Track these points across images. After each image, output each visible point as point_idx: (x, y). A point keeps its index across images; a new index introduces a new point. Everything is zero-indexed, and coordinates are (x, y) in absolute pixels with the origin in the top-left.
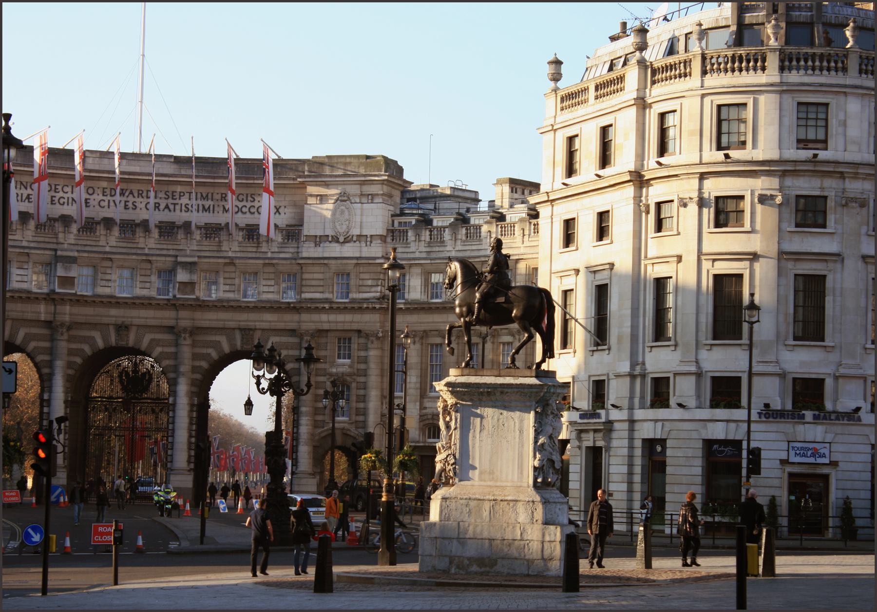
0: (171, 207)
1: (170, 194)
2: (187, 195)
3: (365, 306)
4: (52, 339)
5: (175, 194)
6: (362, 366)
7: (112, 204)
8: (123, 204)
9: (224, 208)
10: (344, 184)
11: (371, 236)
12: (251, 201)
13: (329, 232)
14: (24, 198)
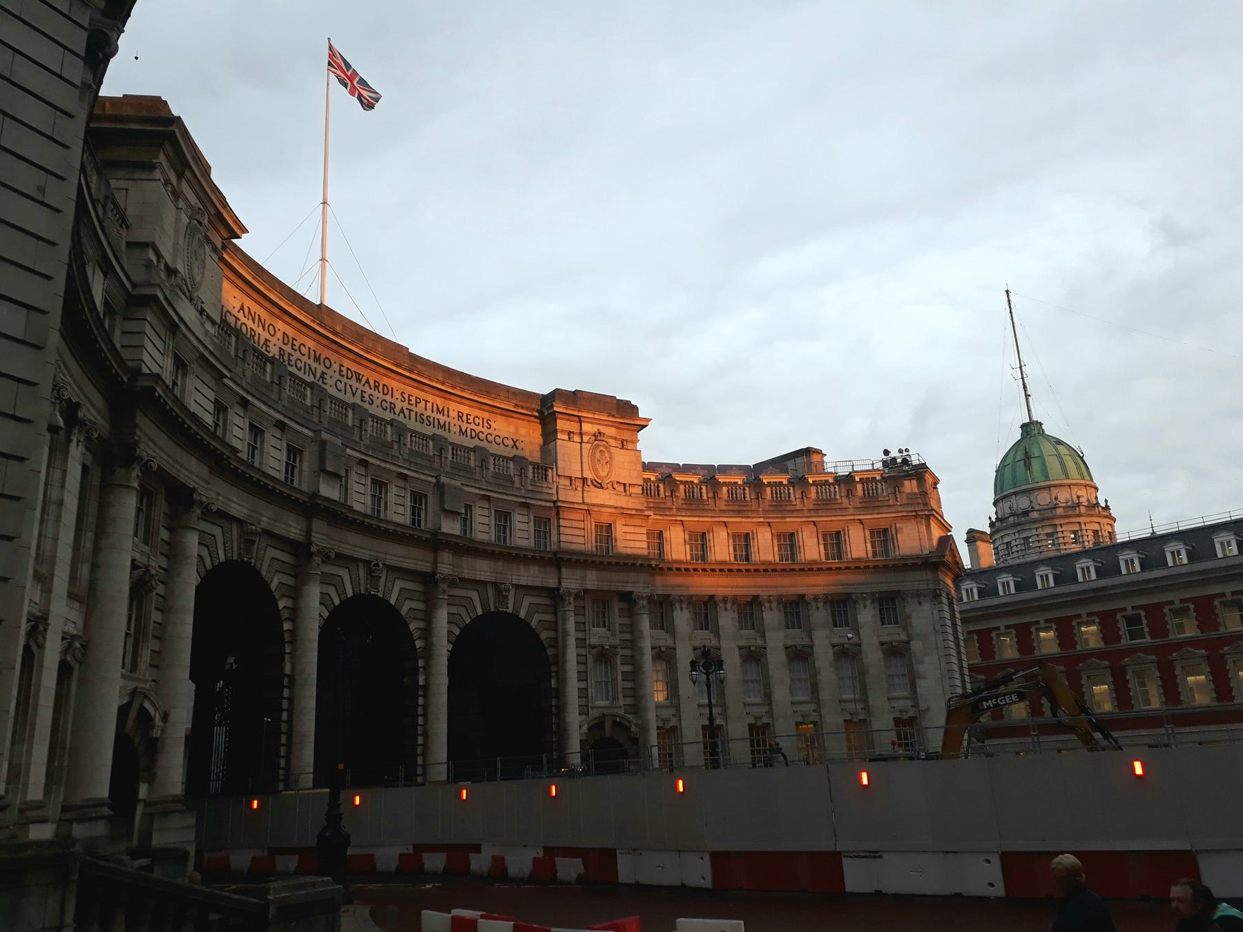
0: (407, 412)
1: (406, 396)
2: (423, 402)
3: (640, 562)
4: (300, 575)
5: (411, 398)
6: (628, 637)
7: (348, 388)
8: (359, 392)
9: (461, 430)
10: (599, 424)
11: (630, 484)
12: (487, 428)
13: (588, 475)
14: (261, 343)
